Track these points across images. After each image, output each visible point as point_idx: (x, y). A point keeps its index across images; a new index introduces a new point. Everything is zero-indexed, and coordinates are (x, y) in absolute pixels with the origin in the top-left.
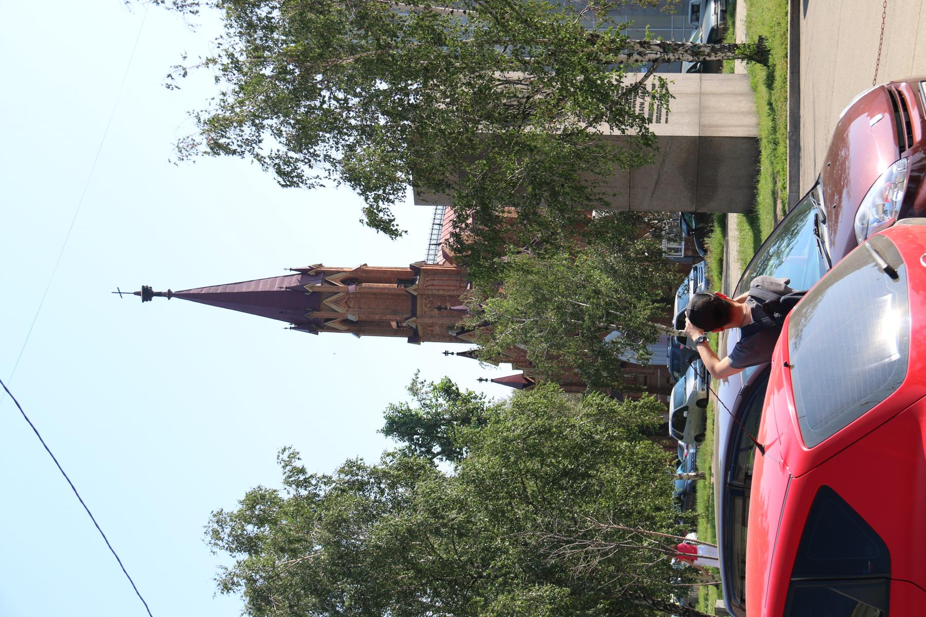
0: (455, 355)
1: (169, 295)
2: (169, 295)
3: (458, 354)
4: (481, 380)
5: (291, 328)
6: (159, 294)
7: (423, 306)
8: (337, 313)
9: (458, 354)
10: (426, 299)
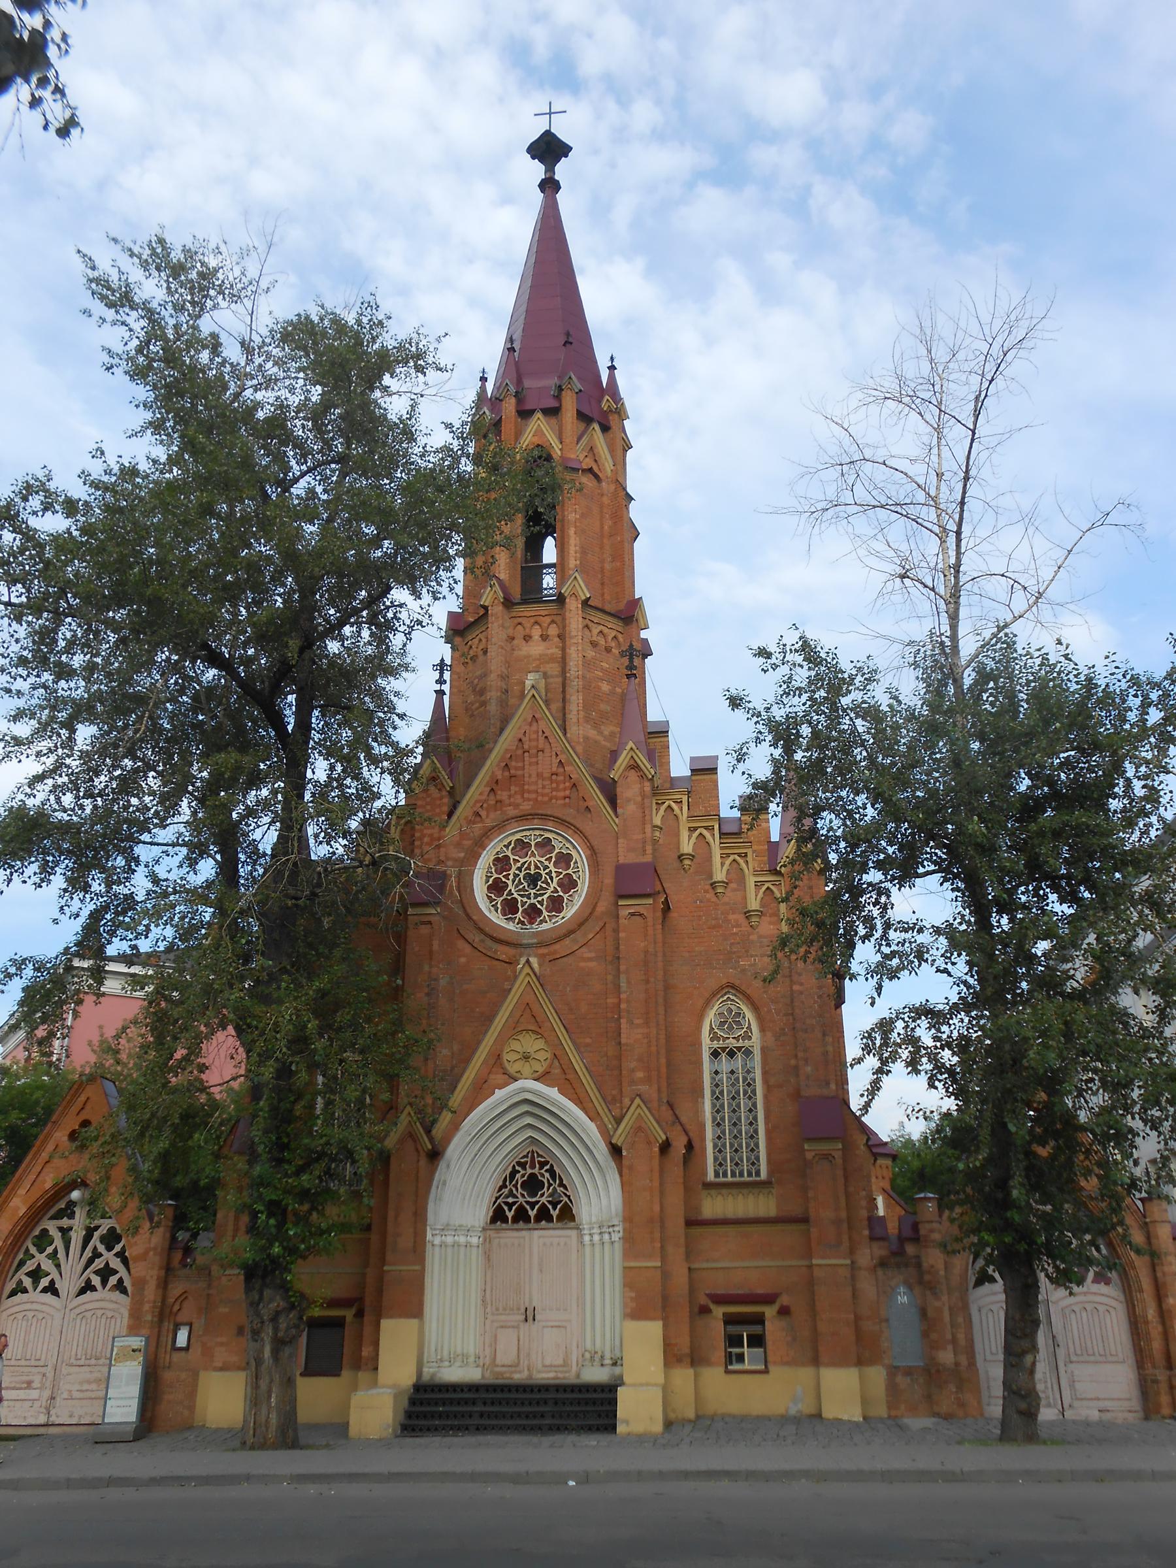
0: (438, 687)
1: (550, 186)
2: (550, 186)
6: (550, 169)
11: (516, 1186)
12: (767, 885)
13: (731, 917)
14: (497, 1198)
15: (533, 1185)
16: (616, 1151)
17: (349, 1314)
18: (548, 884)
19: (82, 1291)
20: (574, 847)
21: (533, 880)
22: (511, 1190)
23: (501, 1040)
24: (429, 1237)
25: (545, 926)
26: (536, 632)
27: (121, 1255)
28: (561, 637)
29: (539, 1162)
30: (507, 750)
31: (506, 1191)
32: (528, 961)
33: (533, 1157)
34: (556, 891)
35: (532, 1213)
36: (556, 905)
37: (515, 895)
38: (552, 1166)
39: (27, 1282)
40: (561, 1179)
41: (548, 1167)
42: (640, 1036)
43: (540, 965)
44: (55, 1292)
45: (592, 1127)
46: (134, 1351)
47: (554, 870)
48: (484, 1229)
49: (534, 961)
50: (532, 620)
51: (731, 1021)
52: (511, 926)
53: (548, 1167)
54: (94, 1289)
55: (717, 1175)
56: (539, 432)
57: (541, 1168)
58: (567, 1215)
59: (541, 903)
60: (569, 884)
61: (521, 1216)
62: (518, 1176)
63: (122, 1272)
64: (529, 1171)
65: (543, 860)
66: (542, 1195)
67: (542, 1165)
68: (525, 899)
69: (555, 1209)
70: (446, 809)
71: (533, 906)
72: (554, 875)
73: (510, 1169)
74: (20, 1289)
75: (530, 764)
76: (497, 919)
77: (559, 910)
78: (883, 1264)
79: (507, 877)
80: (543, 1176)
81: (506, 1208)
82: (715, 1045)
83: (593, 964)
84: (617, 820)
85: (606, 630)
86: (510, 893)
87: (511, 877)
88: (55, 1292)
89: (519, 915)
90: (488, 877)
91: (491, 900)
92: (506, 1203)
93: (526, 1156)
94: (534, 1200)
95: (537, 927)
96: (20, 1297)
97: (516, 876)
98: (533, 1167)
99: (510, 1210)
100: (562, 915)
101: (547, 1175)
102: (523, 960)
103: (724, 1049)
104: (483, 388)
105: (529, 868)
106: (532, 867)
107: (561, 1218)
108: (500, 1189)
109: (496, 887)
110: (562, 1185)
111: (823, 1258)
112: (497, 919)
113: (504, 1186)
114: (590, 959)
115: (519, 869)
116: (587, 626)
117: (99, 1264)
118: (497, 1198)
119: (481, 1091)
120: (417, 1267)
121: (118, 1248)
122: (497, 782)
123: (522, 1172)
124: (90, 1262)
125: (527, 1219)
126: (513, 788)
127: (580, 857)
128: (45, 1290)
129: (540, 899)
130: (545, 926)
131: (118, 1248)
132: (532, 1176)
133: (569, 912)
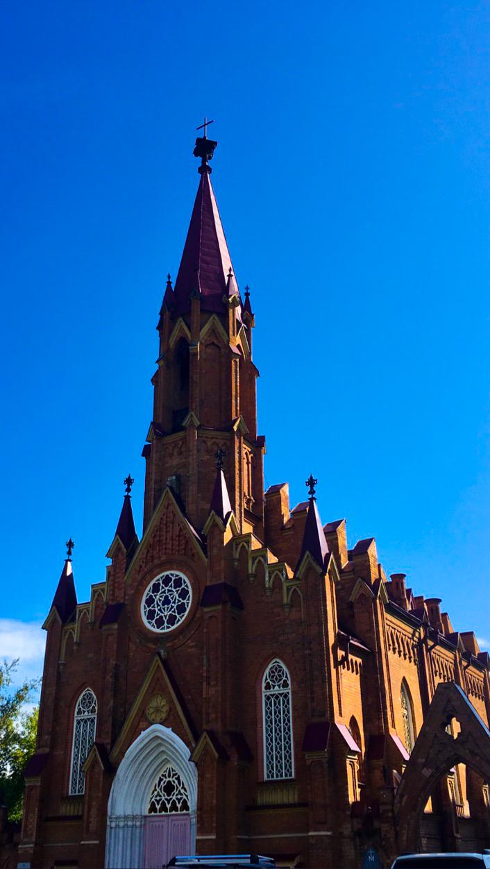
3: (127, 498)
4: (70, 545)
5: (169, 283)
7: (214, 440)
8: (199, 328)
9: (127, 498)
10: (225, 444)
12: (294, 587)
13: (275, 610)
14: (151, 799)
21: (167, 601)
22: (158, 792)
23: (145, 702)
26: (176, 451)
30: (155, 527)
31: (156, 793)
38: (179, 776)
41: (176, 776)
42: (214, 692)
50: (173, 445)
51: (276, 674)
56: (182, 330)
61: (164, 808)
62: (162, 783)
64: (168, 779)
67: (174, 775)
70: (124, 566)
78: (358, 834)
80: (174, 782)
83: (193, 650)
85: (218, 441)
92: (156, 800)
93: (165, 771)
94: (169, 798)
101: (176, 782)
103: (272, 695)
110: (183, 788)
111: (315, 831)
113: (155, 790)
114: (192, 647)
116: (204, 441)
118: (151, 799)
119: (135, 733)
123: (165, 779)
132: (169, 782)
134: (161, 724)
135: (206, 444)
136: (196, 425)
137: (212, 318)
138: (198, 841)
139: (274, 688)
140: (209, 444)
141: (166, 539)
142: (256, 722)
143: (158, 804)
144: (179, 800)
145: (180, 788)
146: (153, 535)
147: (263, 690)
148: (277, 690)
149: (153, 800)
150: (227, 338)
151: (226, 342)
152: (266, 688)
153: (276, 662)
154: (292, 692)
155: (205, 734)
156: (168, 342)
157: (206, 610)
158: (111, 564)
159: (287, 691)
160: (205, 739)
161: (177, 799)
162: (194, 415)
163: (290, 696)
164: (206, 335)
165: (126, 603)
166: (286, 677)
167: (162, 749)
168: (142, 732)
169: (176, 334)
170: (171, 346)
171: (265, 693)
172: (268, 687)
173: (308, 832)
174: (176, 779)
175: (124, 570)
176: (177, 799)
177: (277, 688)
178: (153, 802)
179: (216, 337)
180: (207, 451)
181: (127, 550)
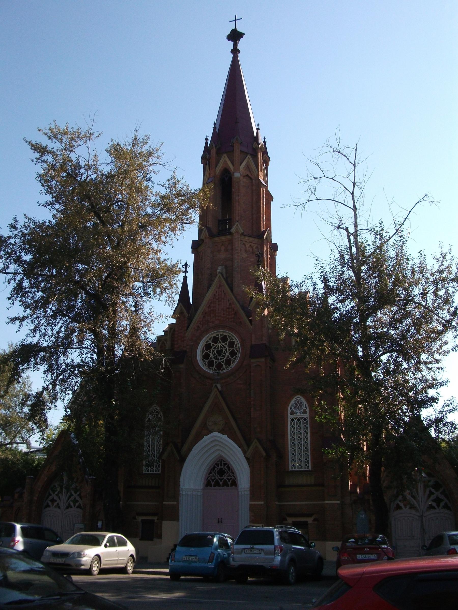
1: (235, 51)
2: (235, 51)
6: (235, 45)
7: (250, 244)
10: (257, 247)
11: (215, 473)
15: (221, 472)
16: (247, 459)
17: (155, 518)
18: (226, 354)
19: (67, 508)
20: (235, 339)
21: (219, 352)
24: (181, 492)
25: (224, 371)
26: (223, 248)
27: (79, 495)
28: (232, 249)
29: (224, 464)
31: (211, 475)
32: (216, 386)
33: (221, 462)
34: (228, 357)
35: (221, 483)
36: (228, 362)
37: (213, 359)
38: (228, 465)
39: (50, 503)
40: (232, 470)
41: (227, 465)
43: (222, 387)
44: (59, 508)
45: (240, 450)
46: (81, 529)
47: (228, 348)
48: (203, 489)
49: (219, 386)
52: (211, 372)
53: (227, 465)
54: (71, 507)
55: (292, 468)
56: (225, 162)
57: (224, 466)
58: (234, 483)
59: (223, 362)
60: (233, 354)
61: (217, 484)
62: (216, 469)
63: (80, 501)
64: (220, 467)
65: (223, 344)
66: (225, 476)
68: (217, 361)
69: (229, 481)
71: (220, 363)
72: (228, 350)
73: (213, 466)
74: (48, 506)
75: (219, 305)
76: (205, 368)
77: (230, 364)
79: (210, 352)
80: (225, 469)
81: (211, 481)
82: (293, 416)
84: (251, 327)
85: (252, 245)
86: (211, 358)
87: (211, 352)
88: (59, 508)
89: (214, 367)
90: (203, 352)
91: (204, 361)
92: (212, 479)
94: (221, 478)
95: (221, 372)
96: (48, 509)
97: (213, 351)
98: (221, 465)
99: (213, 482)
100: (231, 366)
101: (226, 469)
102: (214, 385)
103: (295, 419)
104: (206, 143)
105: (218, 348)
106: (220, 347)
107: (232, 485)
108: (209, 474)
109: (206, 356)
111: (328, 500)
112: (205, 368)
113: (211, 473)
115: (215, 348)
117: (72, 498)
118: (208, 477)
119: (198, 438)
120: (175, 503)
121: (78, 493)
122: (206, 313)
123: (217, 467)
124: (70, 497)
125: (219, 485)
126: (212, 315)
127: (237, 342)
128: (55, 507)
129: (222, 360)
130: (224, 371)
131: (78, 493)
132: (221, 469)
133: (233, 365)
134: (219, 432)
135: (245, 246)
136: (241, 233)
137: (248, 157)
138: (251, 505)
139: (296, 414)
140: (247, 246)
141: (219, 310)
142: (284, 435)
143: (213, 482)
144: (229, 480)
145: (230, 473)
146: (208, 305)
147: (289, 414)
148: (298, 415)
149: (209, 478)
150: (257, 173)
151: (256, 175)
152: (291, 414)
153: (298, 397)
154: (310, 417)
155: (256, 440)
156: (215, 170)
157: (252, 360)
158: (175, 322)
159: (306, 416)
160: (255, 444)
161: (228, 479)
162: (238, 224)
163: (308, 419)
164: (243, 169)
165: (188, 350)
166: (306, 407)
167: (217, 447)
168: (204, 437)
169: (220, 166)
170: (217, 173)
171: (290, 416)
172: (292, 413)
173: (324, 501)
174: (226, 467)
175: (186, 328)
176: (228, 479)
177: (298, 414)
178: (209, 480)
179: (250, 171)
180: (246, 251)
181: (188, 313)
